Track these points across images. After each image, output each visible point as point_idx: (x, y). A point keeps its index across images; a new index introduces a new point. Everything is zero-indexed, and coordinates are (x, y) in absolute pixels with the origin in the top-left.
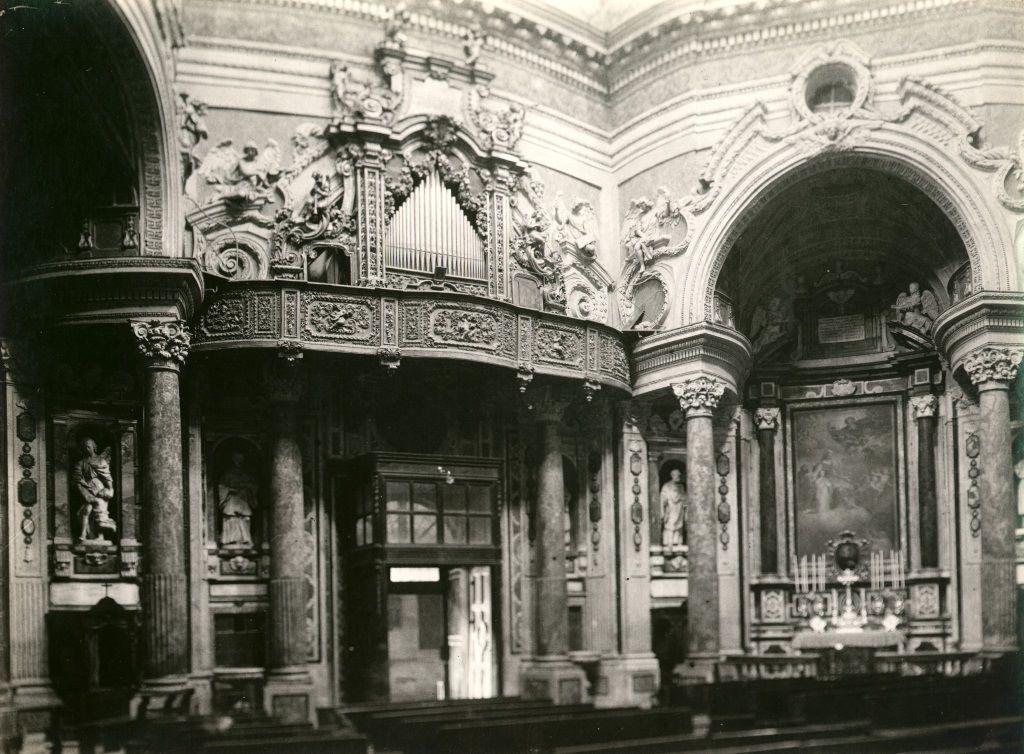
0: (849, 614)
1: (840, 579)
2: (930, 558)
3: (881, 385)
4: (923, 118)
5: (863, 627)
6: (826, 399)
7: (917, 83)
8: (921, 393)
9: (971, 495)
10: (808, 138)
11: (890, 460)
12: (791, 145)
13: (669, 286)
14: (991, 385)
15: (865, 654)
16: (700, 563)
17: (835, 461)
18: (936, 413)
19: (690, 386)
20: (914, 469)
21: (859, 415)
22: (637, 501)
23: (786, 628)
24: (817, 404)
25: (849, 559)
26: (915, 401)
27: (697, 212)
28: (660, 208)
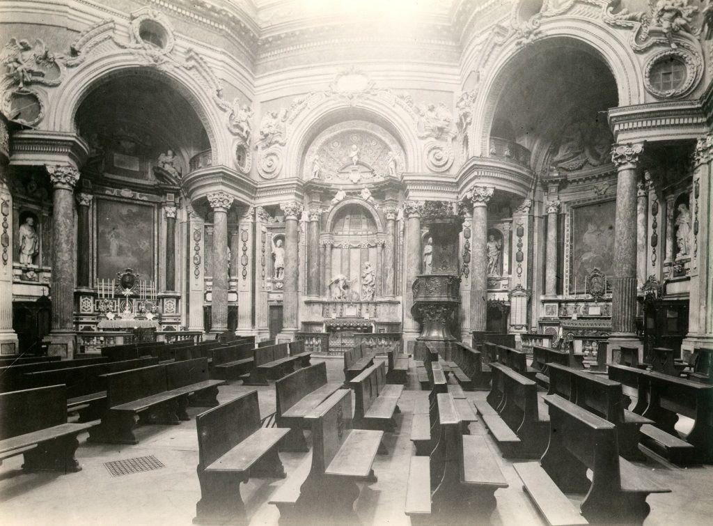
0: (127, 312)
1: (123, 293)
2: (171, 285)
3: (147, 196)
4: (197, 73)
5: (135, 318)
6: (116, 197)
7: (197, 54)
8: (170, 206)
9: (195, 258)
10: (142, 55)
11: (150, 235)
12: (131, 54)
13: (44, 102)
14: (221, 209)
15: (139, 332)
16: (63, 277)
17: (121, 230)
18: (176, 217)
19: (59, 169)
20: (164, 243)
21: (135, 209)
22: (5, 232)
23: (93, 317)
24: (112, 198)
25: (128, 283)
26: (167, 209)
27: (68, 66)
28: (39, 51)
